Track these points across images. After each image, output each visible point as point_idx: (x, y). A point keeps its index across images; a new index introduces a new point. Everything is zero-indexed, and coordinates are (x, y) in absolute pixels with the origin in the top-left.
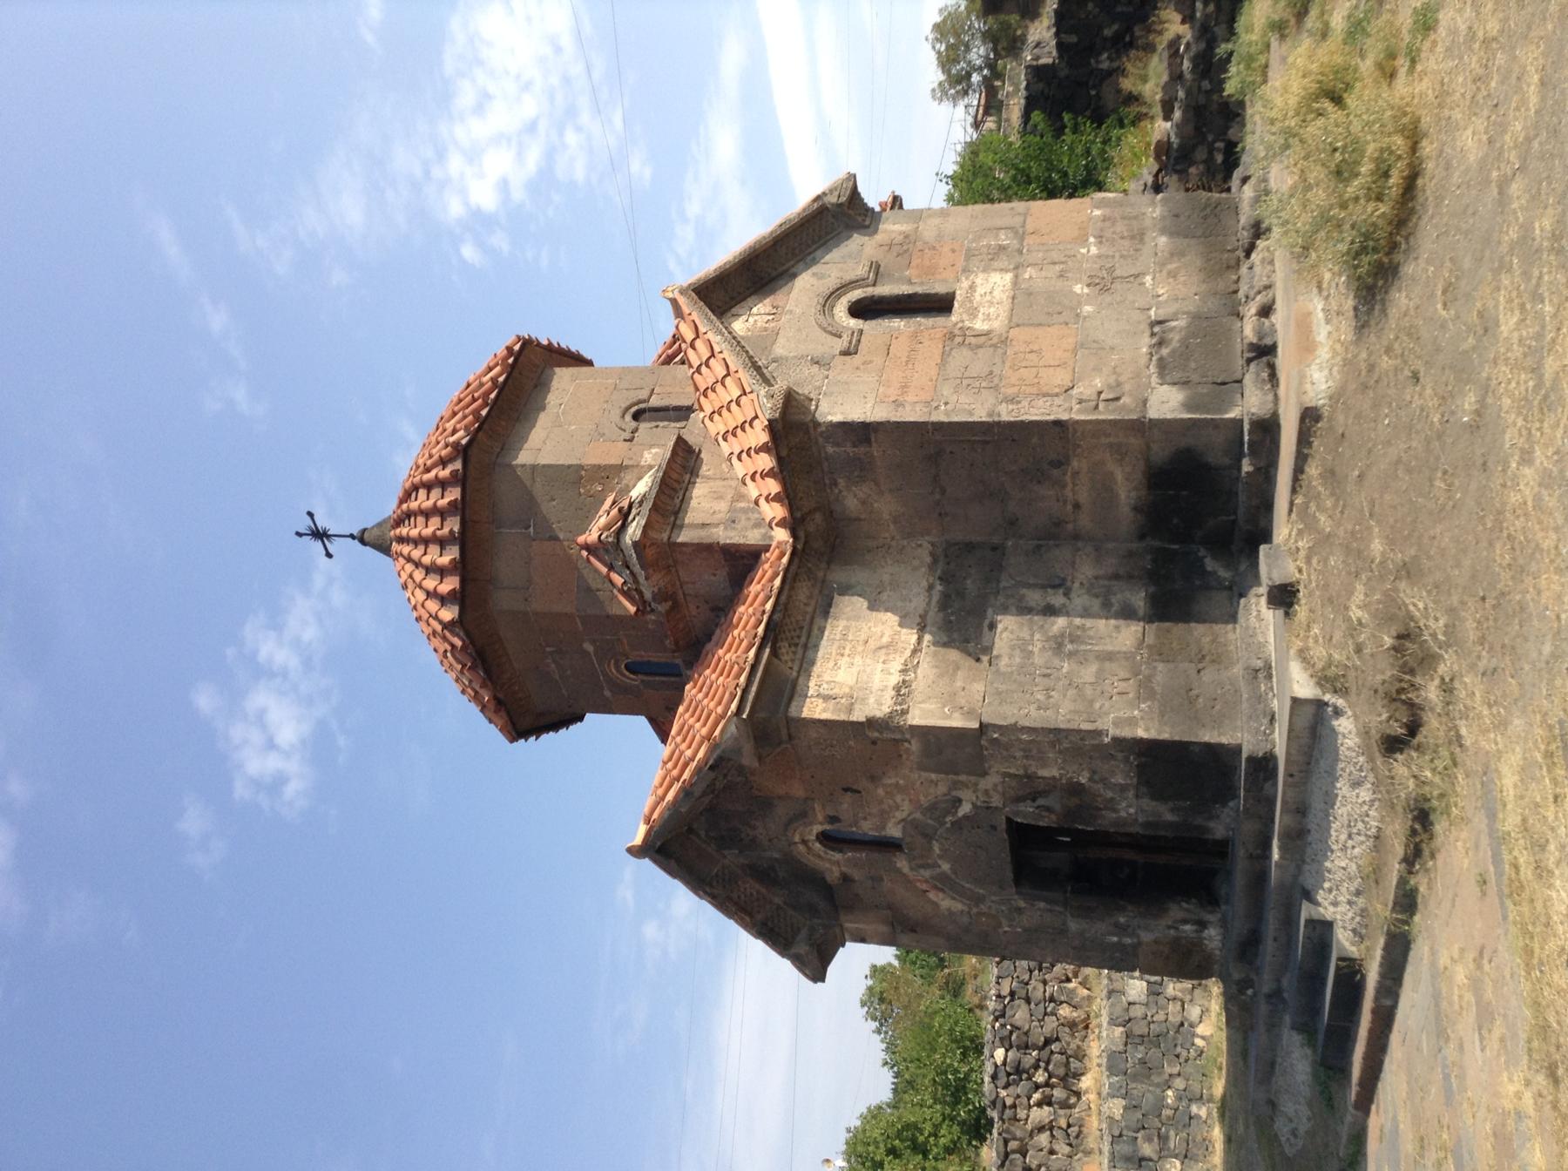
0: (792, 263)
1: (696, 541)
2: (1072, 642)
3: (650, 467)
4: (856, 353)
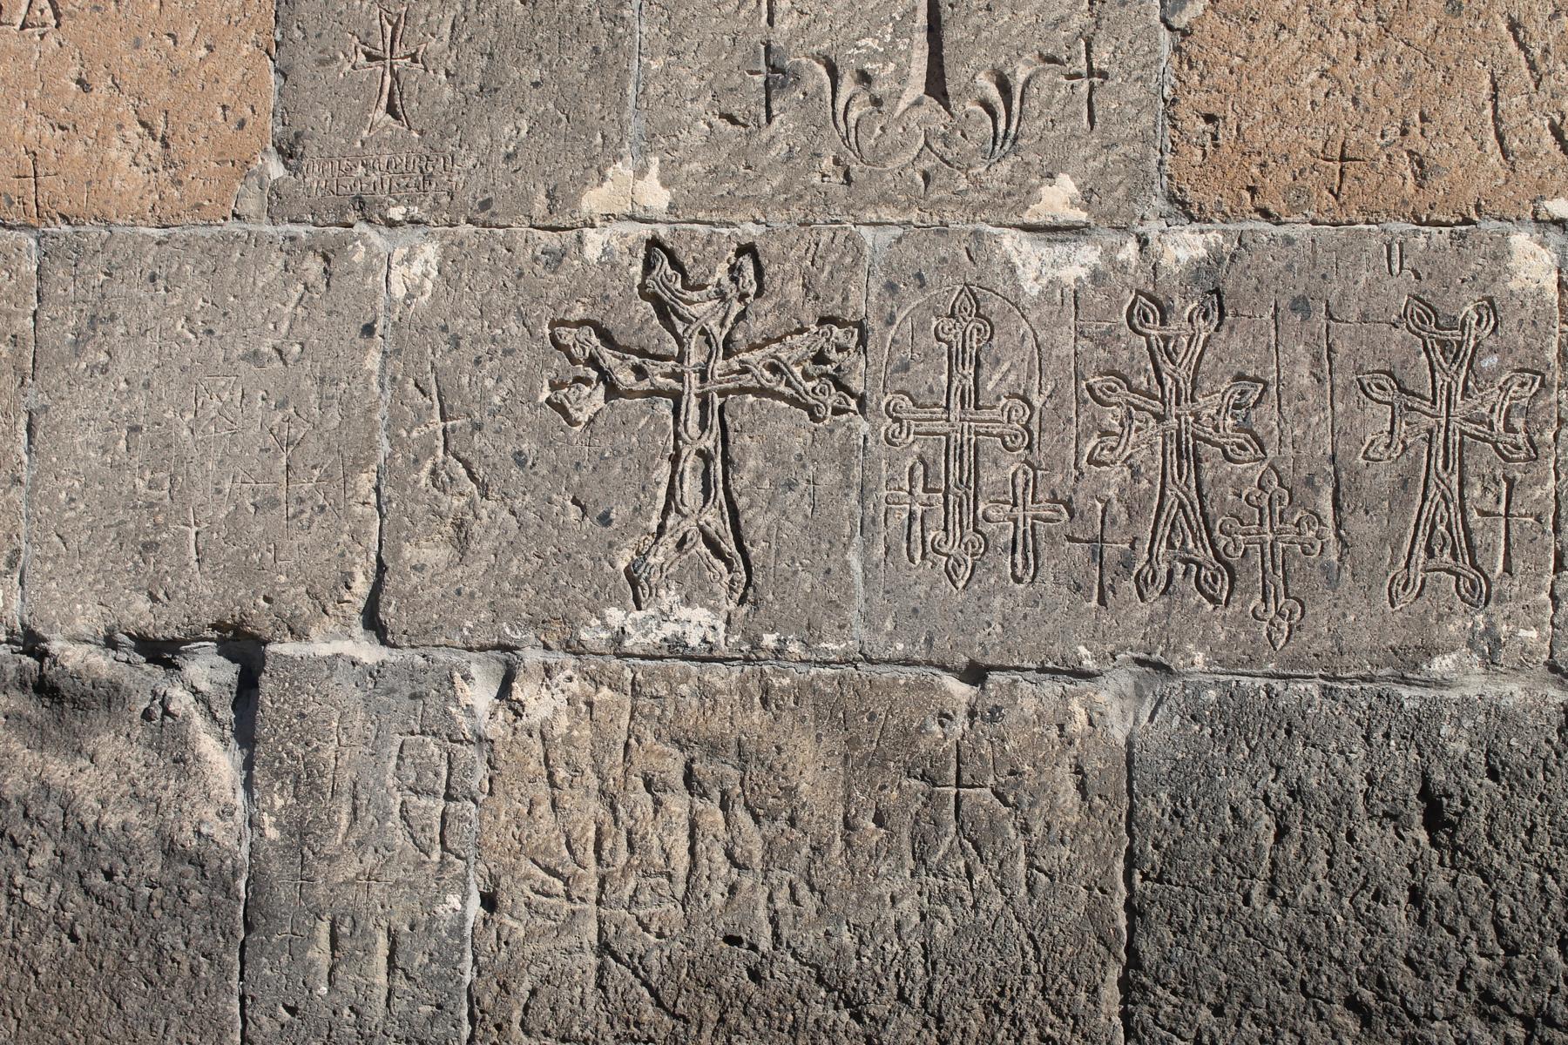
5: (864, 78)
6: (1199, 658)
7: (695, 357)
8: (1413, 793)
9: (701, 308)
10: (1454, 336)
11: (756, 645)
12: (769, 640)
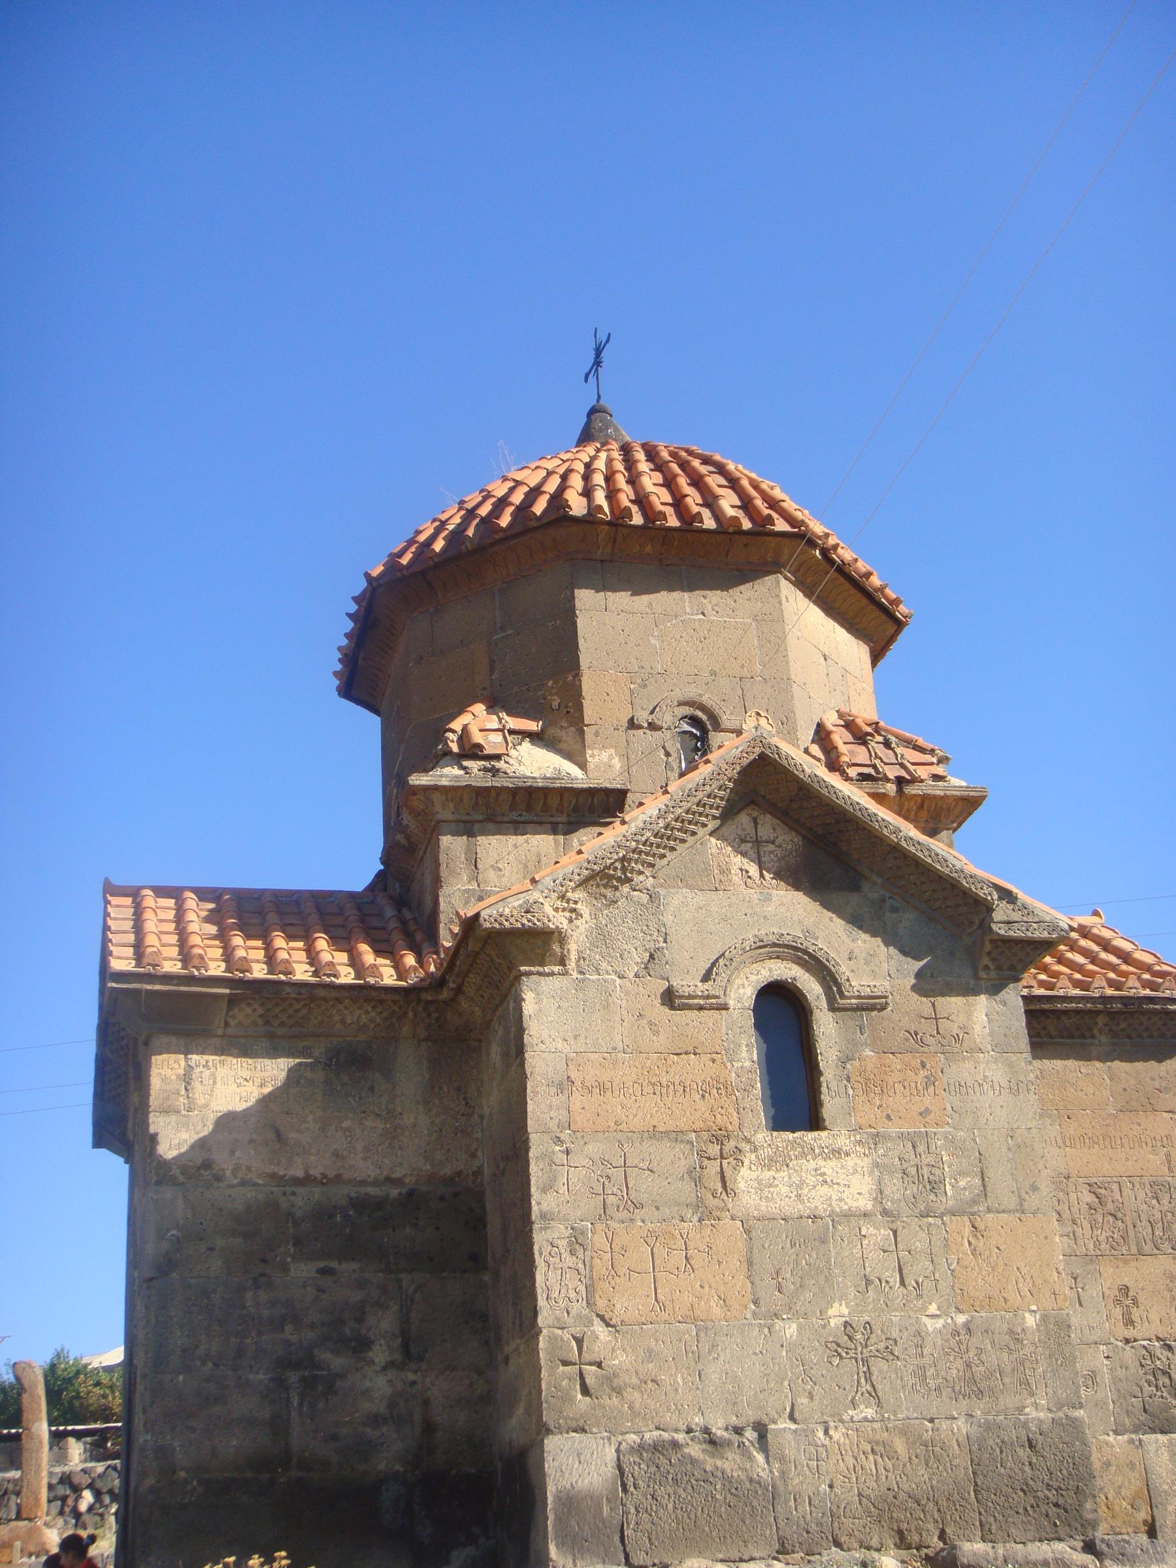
0: (879, 881)
1: (442, 858)
2: (304, 1380)
3: (583, 766)
4: (672, 1008)
5: (887, 1282)
6: (979, 1412)
7: (859, 1349)
8: (1026, 1439)
9: (859, 1336)
10: (1017, 1337)
11: (883, 1416)
12: (886, 1415)
